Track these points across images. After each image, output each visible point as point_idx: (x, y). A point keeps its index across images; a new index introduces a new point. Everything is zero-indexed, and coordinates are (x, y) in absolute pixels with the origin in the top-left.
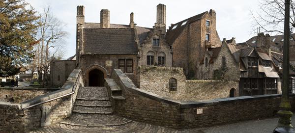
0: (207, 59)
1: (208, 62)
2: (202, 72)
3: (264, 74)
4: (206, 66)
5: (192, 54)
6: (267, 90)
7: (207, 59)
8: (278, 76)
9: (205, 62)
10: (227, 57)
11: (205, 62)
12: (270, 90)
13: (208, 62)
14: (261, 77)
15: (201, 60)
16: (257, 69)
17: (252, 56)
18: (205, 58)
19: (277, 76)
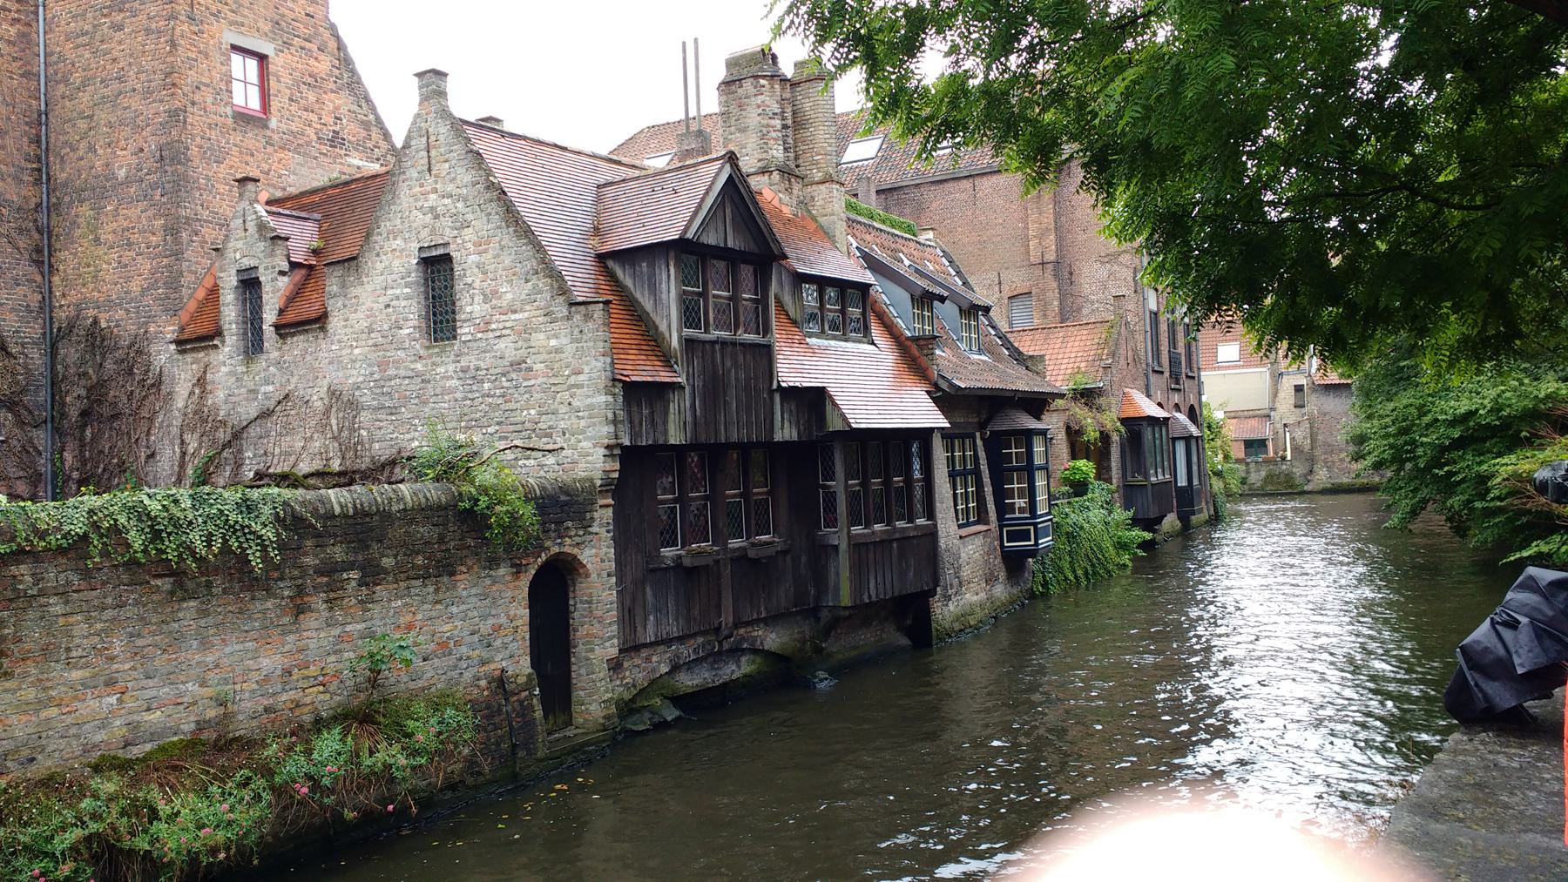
0: (250, 284)
1: (269, 317)
2: (201, 418)
3: (814, 401)
4: (253, 345)
5: (84, 245)
6: (857, 546)
7: (250, 284)
8: (940, 421)
9: (230, 313)
10: (467, 262)
11: (230, 313)
12: (884, 543)
13: (269, 317)
14: (785, 432)
15: (192, 296)
16: (764, 355)
17: (711, 239)
18: (230, 281)
19: (931, 417)
